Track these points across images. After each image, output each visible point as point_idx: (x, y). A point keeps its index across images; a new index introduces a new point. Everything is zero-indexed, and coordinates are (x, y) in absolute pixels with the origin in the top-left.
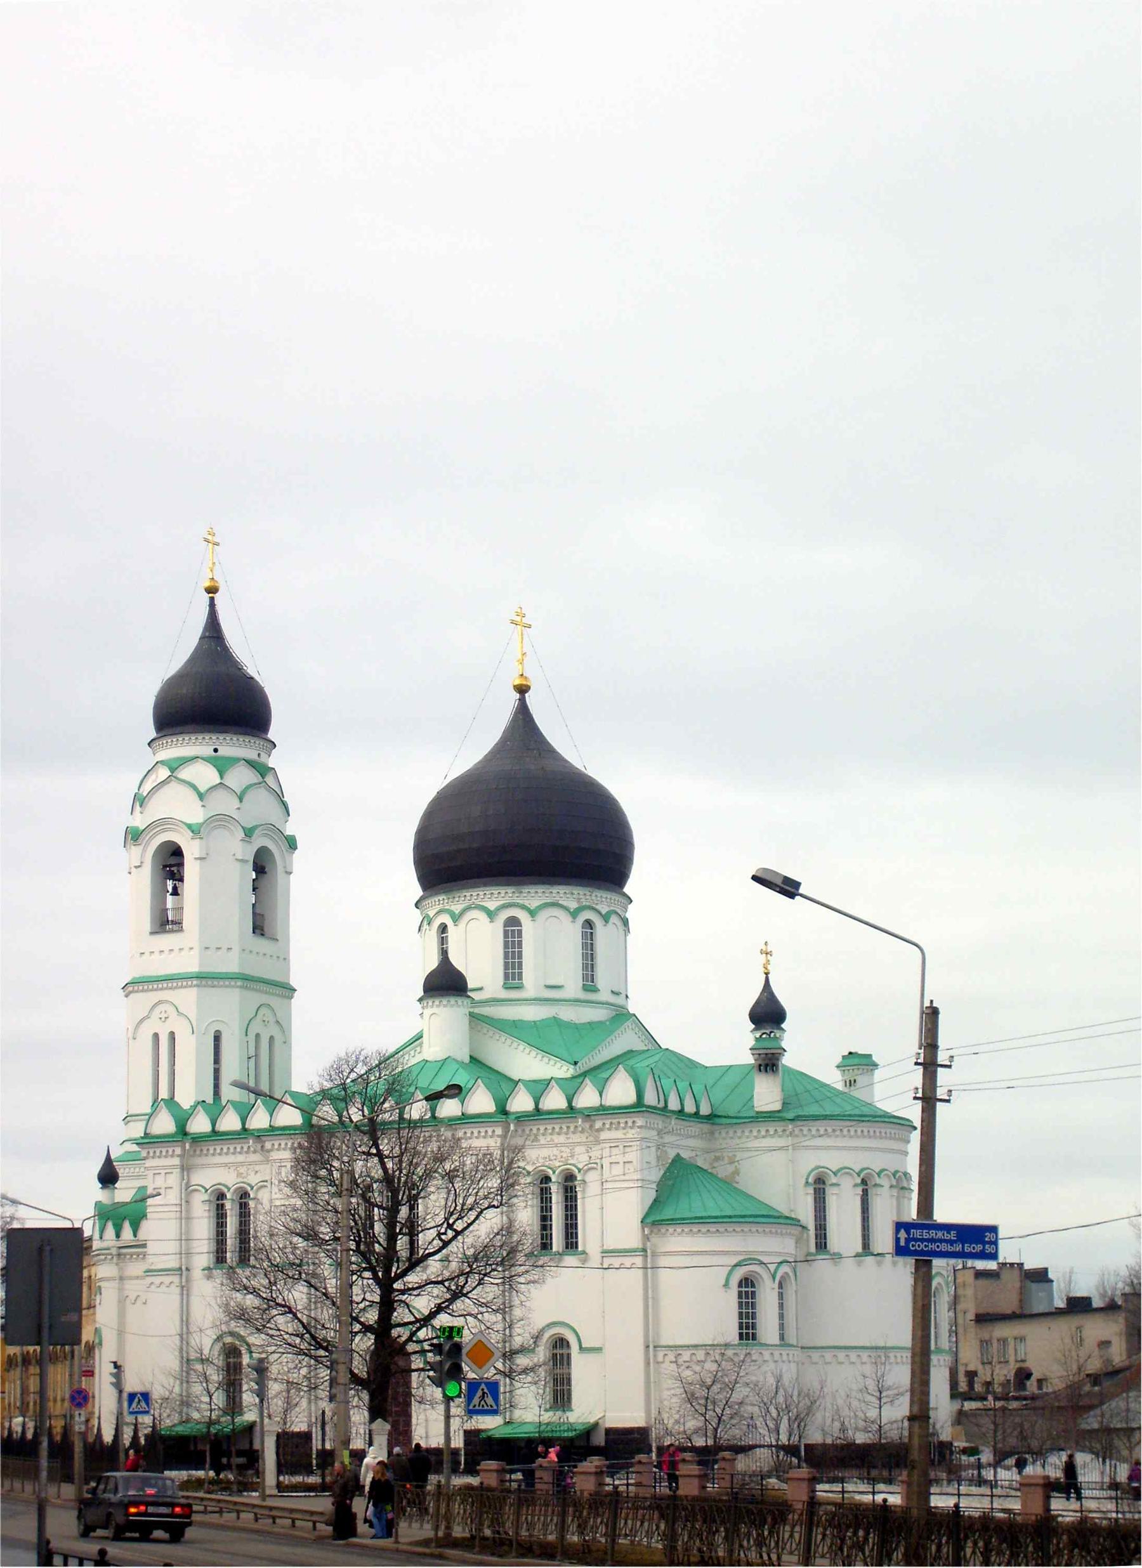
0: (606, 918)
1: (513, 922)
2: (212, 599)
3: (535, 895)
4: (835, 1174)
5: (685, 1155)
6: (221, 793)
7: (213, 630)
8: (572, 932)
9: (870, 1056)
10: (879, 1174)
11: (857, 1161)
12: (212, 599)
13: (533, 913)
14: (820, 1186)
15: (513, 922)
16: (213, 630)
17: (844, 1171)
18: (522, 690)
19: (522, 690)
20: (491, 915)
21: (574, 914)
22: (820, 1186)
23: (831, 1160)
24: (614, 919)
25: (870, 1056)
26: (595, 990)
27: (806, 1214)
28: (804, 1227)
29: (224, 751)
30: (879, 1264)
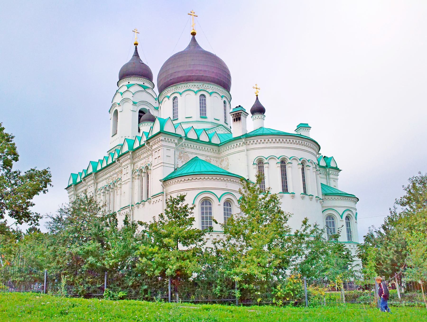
0: (210, 94)
1: (175, 98)
5: (200, 157)
6: (127, 93)
7: (136, 54)
8: (196, 99)
11: (279, 153)
13: (181, 94)
14: (260, 163)
15: (175, 98)
16: (136, 54)
17: (272, 158)
18: (194, 34)
19: (194, 34)
20: (169, 98)
21: (196, 93)
22: (260, 163)
23: (265, 153)
29: (131, 82)
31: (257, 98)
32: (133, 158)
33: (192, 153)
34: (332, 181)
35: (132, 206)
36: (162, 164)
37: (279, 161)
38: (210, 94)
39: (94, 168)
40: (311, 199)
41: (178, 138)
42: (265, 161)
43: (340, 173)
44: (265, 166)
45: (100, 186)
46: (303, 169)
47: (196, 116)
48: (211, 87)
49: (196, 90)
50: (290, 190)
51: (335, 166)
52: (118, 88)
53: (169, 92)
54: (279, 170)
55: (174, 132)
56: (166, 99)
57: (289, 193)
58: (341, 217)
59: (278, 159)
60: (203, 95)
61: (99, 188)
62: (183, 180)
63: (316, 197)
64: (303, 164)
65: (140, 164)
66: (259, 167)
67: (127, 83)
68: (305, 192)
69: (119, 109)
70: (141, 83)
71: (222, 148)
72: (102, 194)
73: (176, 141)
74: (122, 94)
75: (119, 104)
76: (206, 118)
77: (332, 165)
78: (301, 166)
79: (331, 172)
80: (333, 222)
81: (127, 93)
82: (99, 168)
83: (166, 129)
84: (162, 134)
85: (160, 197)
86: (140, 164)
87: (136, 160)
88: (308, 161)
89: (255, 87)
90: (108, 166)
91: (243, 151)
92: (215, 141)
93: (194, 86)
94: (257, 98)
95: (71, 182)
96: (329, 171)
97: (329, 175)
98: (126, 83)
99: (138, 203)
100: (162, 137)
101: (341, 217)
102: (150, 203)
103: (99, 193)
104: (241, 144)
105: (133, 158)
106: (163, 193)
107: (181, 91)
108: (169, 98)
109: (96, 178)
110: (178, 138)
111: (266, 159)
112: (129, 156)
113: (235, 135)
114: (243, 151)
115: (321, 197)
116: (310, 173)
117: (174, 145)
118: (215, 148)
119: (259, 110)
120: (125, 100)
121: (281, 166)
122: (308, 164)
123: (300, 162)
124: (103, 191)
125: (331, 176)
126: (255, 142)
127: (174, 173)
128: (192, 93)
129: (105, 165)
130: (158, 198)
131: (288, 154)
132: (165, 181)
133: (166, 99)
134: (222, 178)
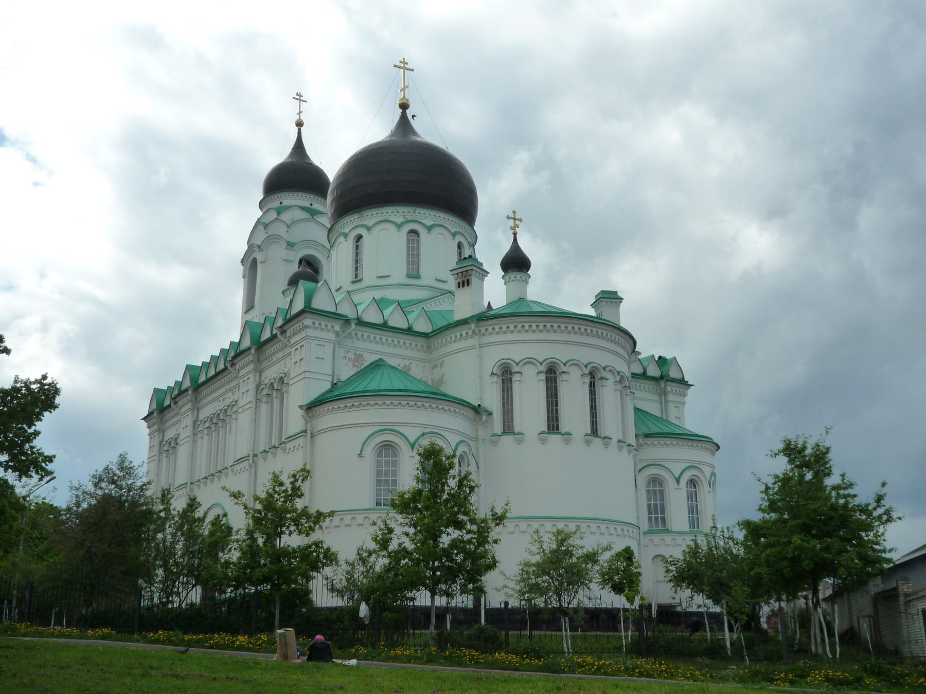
0: (429, 229)
2: (299, 133)
3: (371, 216)
4: (517, 364)
7: (299, 147)
8: (401, 238)
9: (616, 292)
10: (565, 365)
11: (543, 353)
12: (299, 133)
13: (369, 229)
14: (506, 374)
15: (359, 238)
16: (299, 147)
17: (529, 362)
21: (399, 226)
22: (506, 374)
23: (515, 353)
24: (436, 231)
25: (616, 292)
26: (418, 277)
27: (492, 400)
28: (477, 410)
29: (286, 202)
30: (567, 442)
31: (515, 240)
32: (258, 361)
33: (371, 352)
34: (671, 407)
35: (255, 455)
36: (306, 375)
37: (543, 368)
38: (429, 229)
39: (194, 380)
40: (606, 445)
41: (342, 322)
42: (516, 369)
43: (690, 391)
44: (516, 378)
45: (205, 413)
46: (592, 385)
47: (399, 273)
48: (428, 216)
49: (399, 220)
50: (563, 428)
51: (679, 377)
52: (260, 213)
53: (350, 223)
54: (542, 386)
55: (333, 310)
56: (342, 239)
57: (560, 433)
58: (678, 481)
59: (541, 364)
60: (414, 232)
61: (201, 418)
62: (342, 406)
63: (619, 441)
64: (592, 375)
65: (271, 374)
66: (503, 380)
67: (276, 204)
68: (595, 431)
69: (259, 257)
70: (306, 204)
71: (435, 342)
72: (206, 432)
73: (337, 328)
74: (266, 226)
75: (259, 247)
76: (418, 277)
77: (673, 374)
78: (587, 380)
79: (669, 389)
80: (662, 492)
81: (277, 224)
82: (202, 379)
83: (317, 304)
84: (307, 315)
85: (300, 441)
86: (271, 374)
87: (265, 364)
88: (604, 368)
89: (512, 215)
90: (217, 374)
91: (472, 348)
92: (422, 326)
93: (396, 213)
94: (515, 240)
95: (154, 406)
96: (665, 386)
97: (665, 394)
98: (276, 204)
99: (265, 451)
100: (308, 321)
101: (678, 481)
102: (284, 450)
103: (200, 428)
104: (470, 333)
105: (258, 361)
106: (305, 431)
107: (370, 222)
108: (346, 236)
109: (196, 400)
110: (342, 322)
111: (517, 364)
112: (251, 357)
113: (458, 316)
114: (472, 348)
115: (632, 440)
116: (608, 394)
117: (332, 336)
118: (421, 341)
119: (516, 263)
120: (272, 239)
121: (547, 378)
122: (604, 374)
123: (587, 372)
124: (207, 425)
125: (670, 397)
126: (497, 330)
127: (330, 391)
128: (392, 228)
129: (212, 372)
130: (296, 443)
131: (561, 354)
132: (311, 408)
133: (342, 239)
134: (419, 404)
